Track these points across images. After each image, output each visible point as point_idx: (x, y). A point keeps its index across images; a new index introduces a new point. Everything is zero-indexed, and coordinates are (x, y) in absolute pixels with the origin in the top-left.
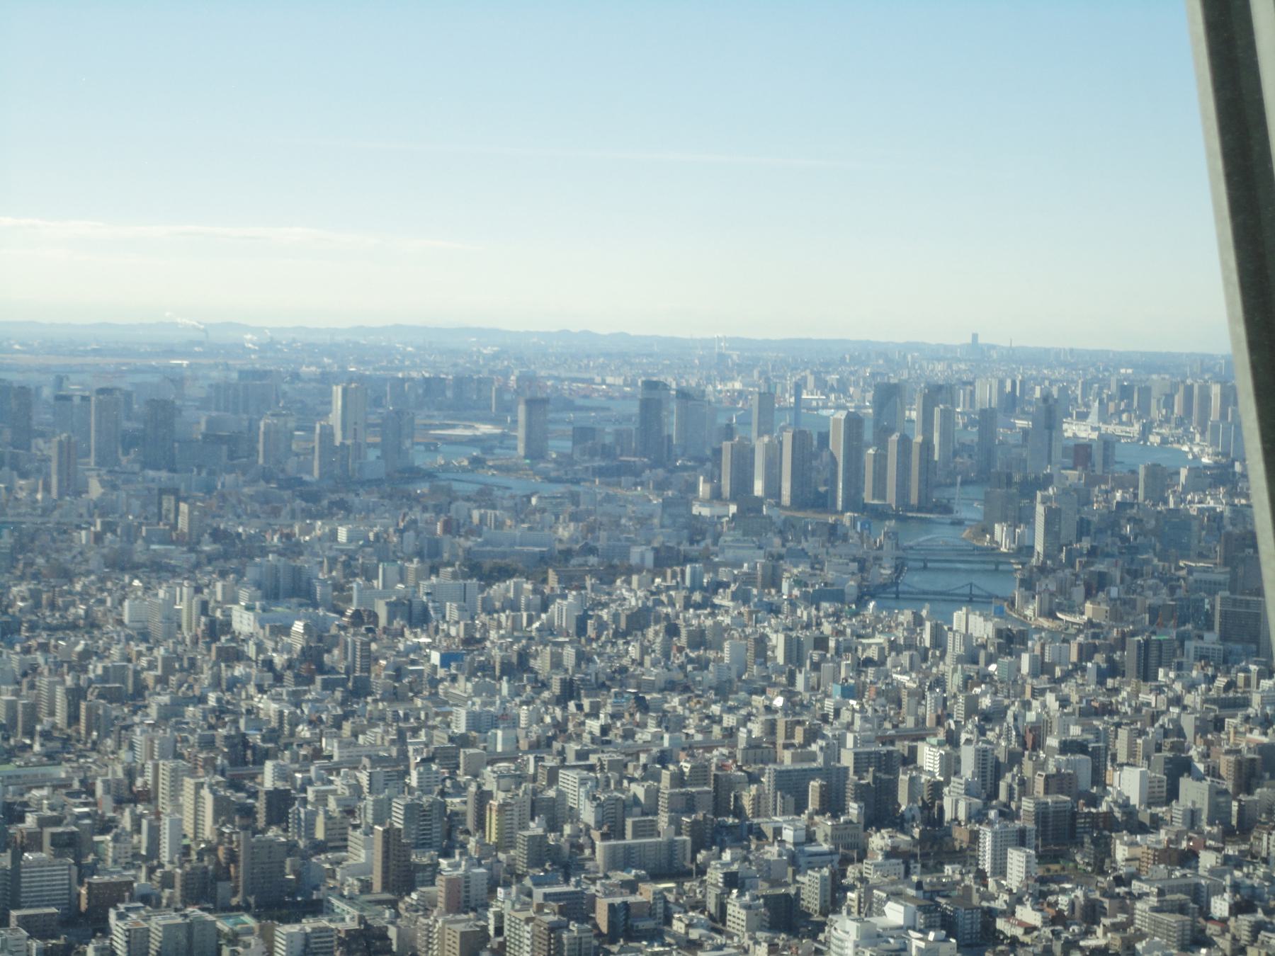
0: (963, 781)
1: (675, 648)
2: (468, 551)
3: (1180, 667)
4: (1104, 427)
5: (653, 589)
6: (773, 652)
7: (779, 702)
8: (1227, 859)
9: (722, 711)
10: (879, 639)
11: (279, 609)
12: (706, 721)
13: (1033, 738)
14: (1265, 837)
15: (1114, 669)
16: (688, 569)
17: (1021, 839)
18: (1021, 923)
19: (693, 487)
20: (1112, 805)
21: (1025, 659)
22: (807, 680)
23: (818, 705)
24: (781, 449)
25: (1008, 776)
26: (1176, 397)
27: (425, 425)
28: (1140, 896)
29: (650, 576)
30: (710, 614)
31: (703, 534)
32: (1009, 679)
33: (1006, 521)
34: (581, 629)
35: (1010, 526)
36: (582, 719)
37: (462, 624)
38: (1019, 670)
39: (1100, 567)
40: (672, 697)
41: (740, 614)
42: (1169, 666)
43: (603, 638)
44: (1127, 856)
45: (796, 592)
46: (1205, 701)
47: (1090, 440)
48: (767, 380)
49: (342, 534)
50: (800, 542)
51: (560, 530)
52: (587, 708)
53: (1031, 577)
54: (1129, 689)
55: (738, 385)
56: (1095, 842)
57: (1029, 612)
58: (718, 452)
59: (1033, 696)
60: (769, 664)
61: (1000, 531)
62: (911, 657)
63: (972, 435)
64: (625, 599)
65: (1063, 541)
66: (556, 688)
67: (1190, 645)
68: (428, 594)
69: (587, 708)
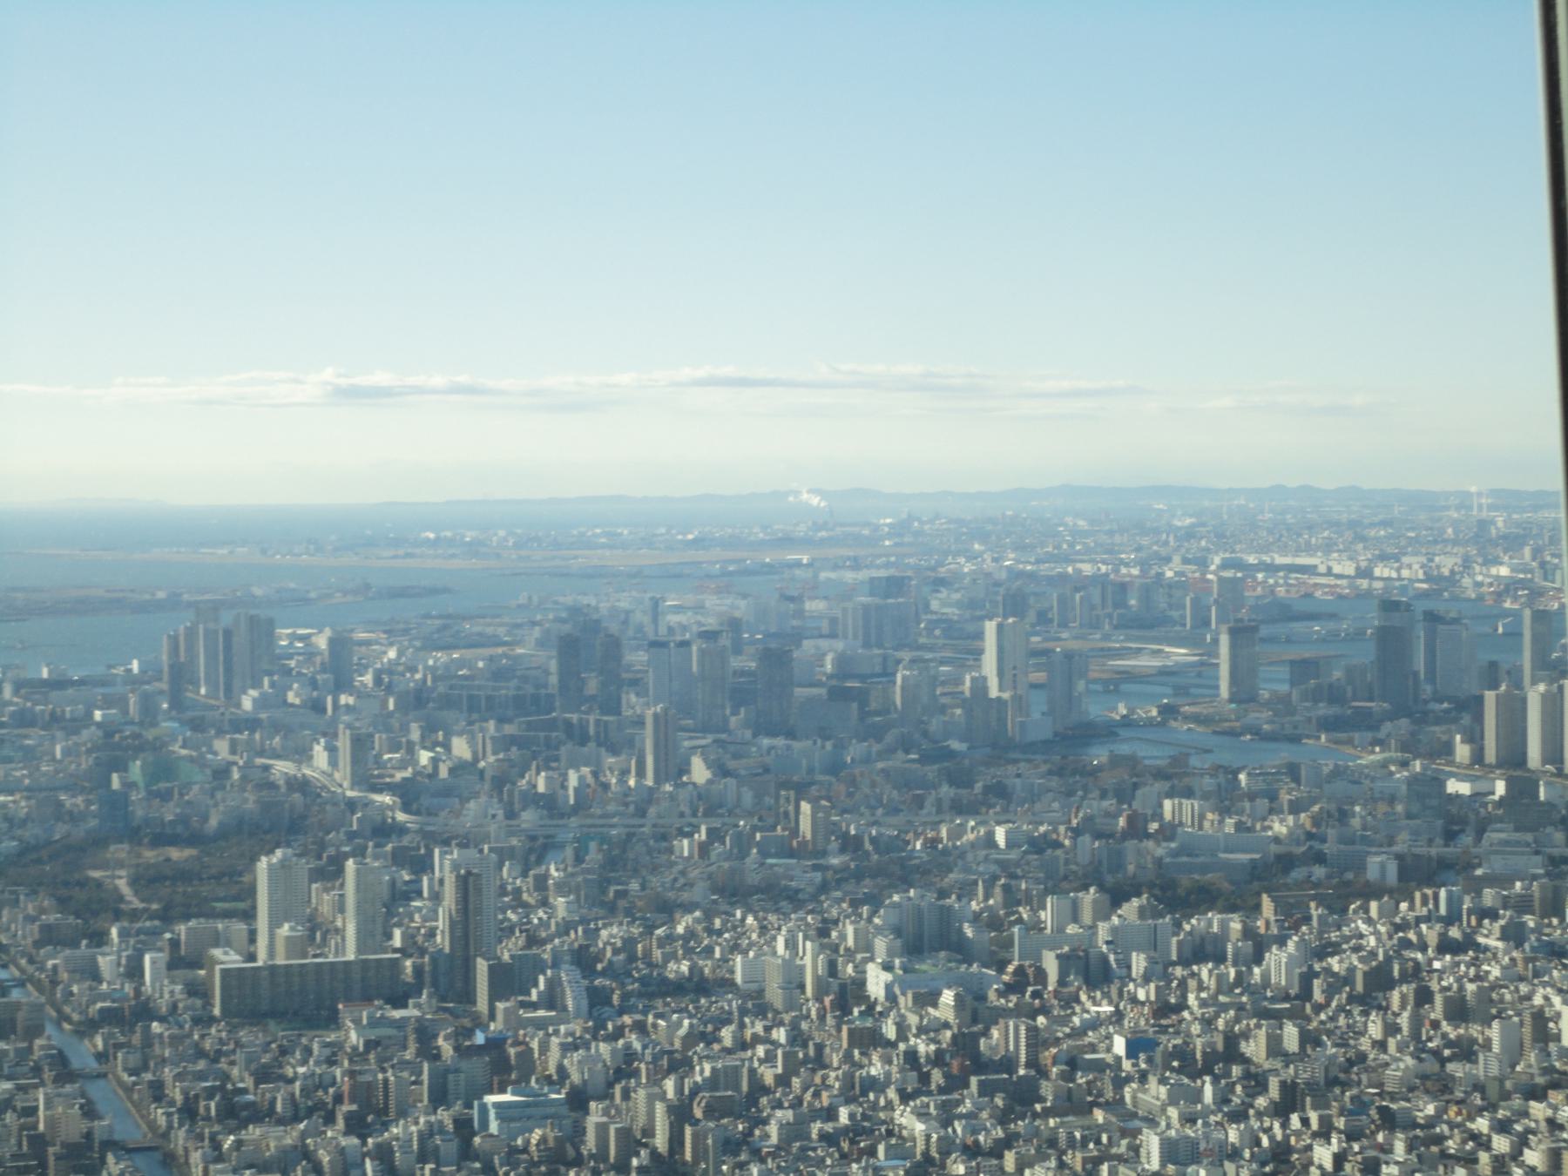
1: (1427, 1023)
2: (1159, 862)
5: (1398, 920)
6: (1556, 1023)
9: (1492, 1128)
11: (924, 967)
12: (1471, 1143)
16: (1443, 893)
19: (1448, 749)
27: (1102, 649)
31: (1463, 821)
36: (1309, 1141)
37: (1152, 986)
40: (1426, 1103)
41: (1513, 960)
43: (1334, 1004)
48: (1543, 564)
49: (1000, 835)
52: (1315, 1125)
55: (1504, 571)
58: (1480, 700)
60: (1552, 1047)
64: (1361, 936)
66: (1274, 1091)
68: (1108, 943)
69: (1315, 1125)
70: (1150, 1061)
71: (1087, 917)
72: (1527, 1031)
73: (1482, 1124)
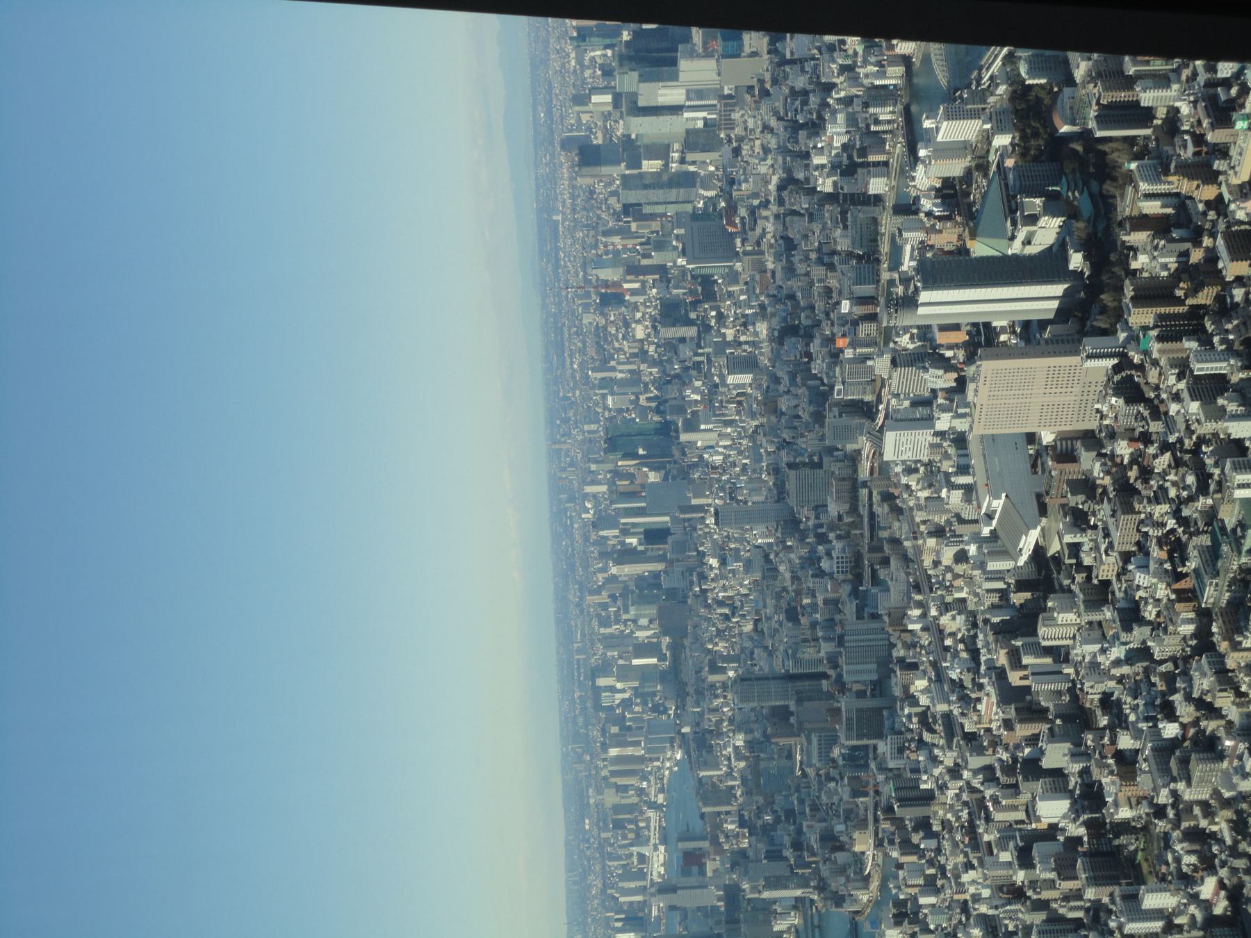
3: (916, 770)
4: (652, 841)
13: (1017, 894)
14: (1089, 697)
15: (923, 825)
17: (1132, 899)
18: (1216, 894)
20: (1078, 823)
21: (923, 901)
25: (1061, 911)
26: (619, 783)
28: (1175, 794)
32: (947, 913)
33: (771, 922)
35: (775, 918)
38: (933, 906)
39: (813, 839)
44: (1127, 808)
46: (950, 748)
47: (666, 851)
53: (831, 899)
54: (941, 813)
56: (1117, 836)
57: (865, 898)
65: (788, 873)
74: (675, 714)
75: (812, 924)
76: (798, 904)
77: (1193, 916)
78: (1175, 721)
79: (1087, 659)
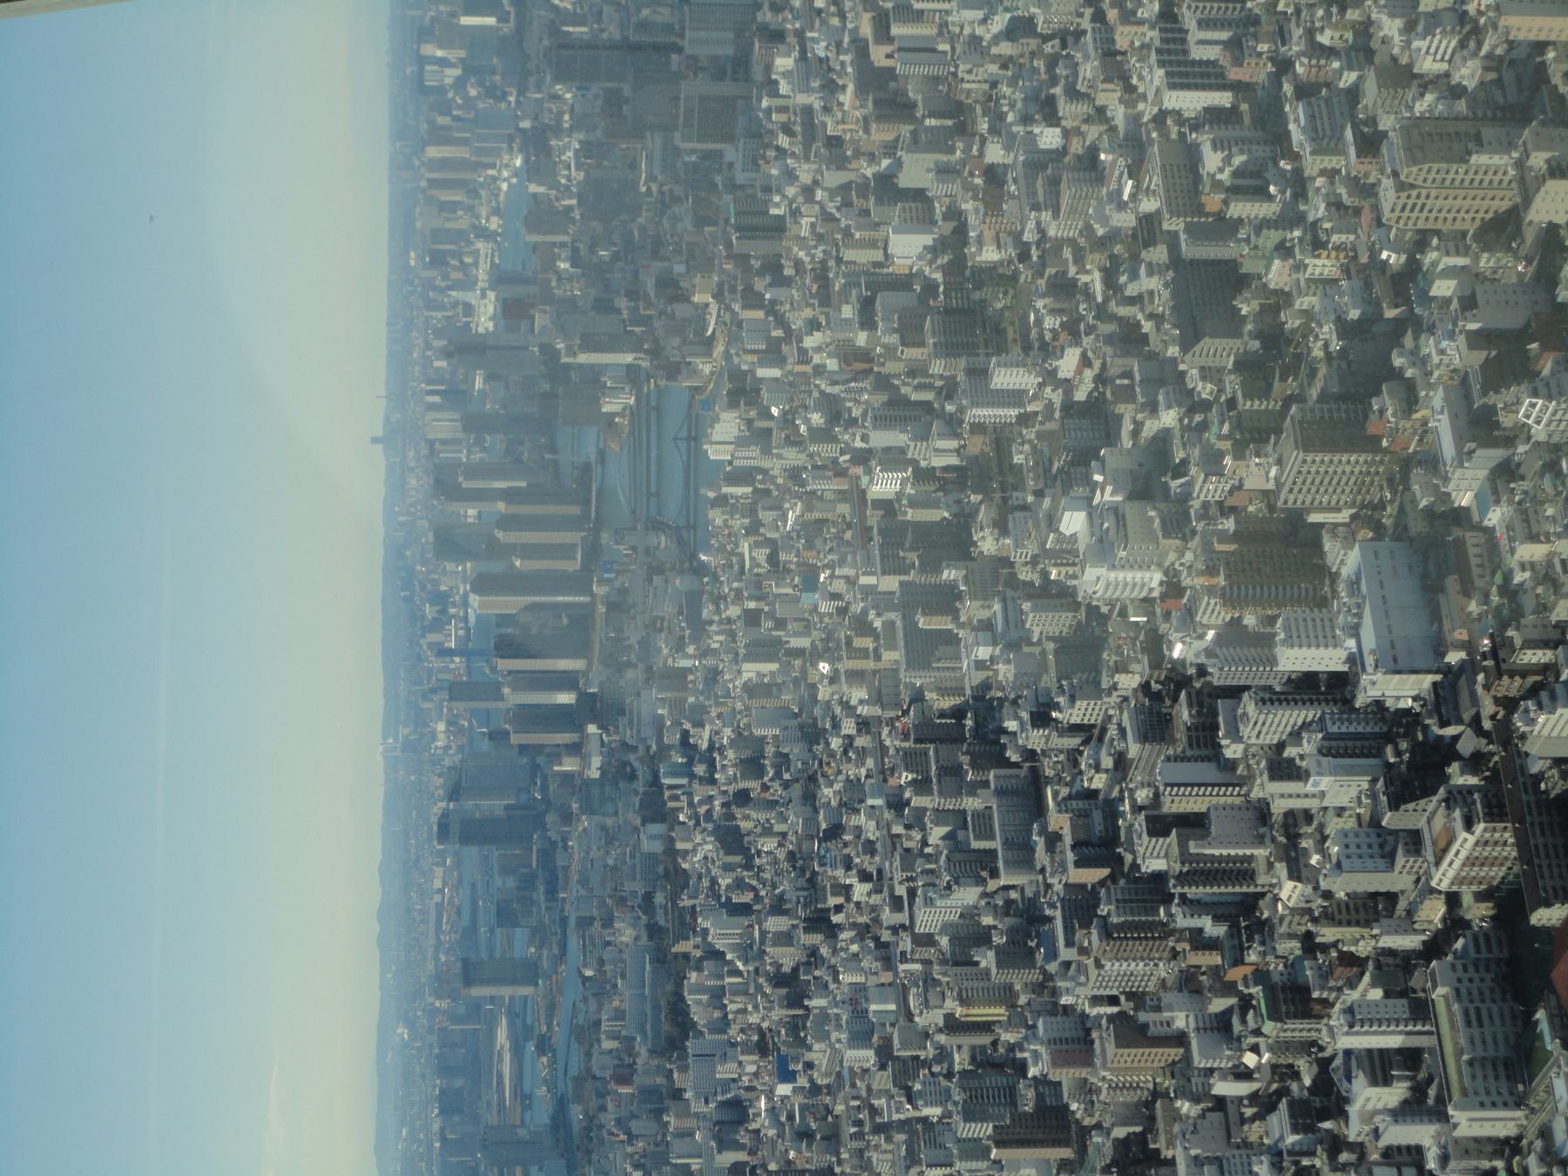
0: (912, 444)
2: (652, 1052)
3: (767, 190)
5: (692, 823)
7: (824, 667)
8: (994, 131)
9: (838, 735)
10: (745, 547)
13: (858, 362)
14: (966, 86)
15: (773, 267)
16: (667, 781)
17: (980, 374)
18: (1079, 372)
19: (567, 777)
21: (762, 372)
22: (796, 634)
23: (826, 619)
24: (518, 672)
25: (903, 390)
26: (443, 198)
28: (1041, 231)
29: (677, 828)
30: (721, 754)
31: (625, 764)
34: (745, 909)
37: (741, 1058)
38: (776, 380)
39: (650, 285)
42: (767, 203)
43: (754, 883)
45: (691, 650)
46: (807, 159)
48: (434, 691)
50: (630, 647)
51: (624, 939)
52: (840, 900)
54: (796, 249)
55: (441, 727)
56: (979, 286)
57: (707, 369)
58: (523, 749)
59: (808, 362)
60: (779, 681)
61: (610, 406)
62: (764, 509)
63: (496, 442)
64: (706, 858)
66: (817, 938)
67: (741, 177)
68: (707, 1102)
69: (840, 900)
70: (796, 1059)
71: (689, 1123)
72: (763, 702)
73: (836, 743)
74: (517, 102)
75: (648, 404)
76: (632, 375)
77: (1050, 406)
78: (1057, 125)
79: (967, 31)
